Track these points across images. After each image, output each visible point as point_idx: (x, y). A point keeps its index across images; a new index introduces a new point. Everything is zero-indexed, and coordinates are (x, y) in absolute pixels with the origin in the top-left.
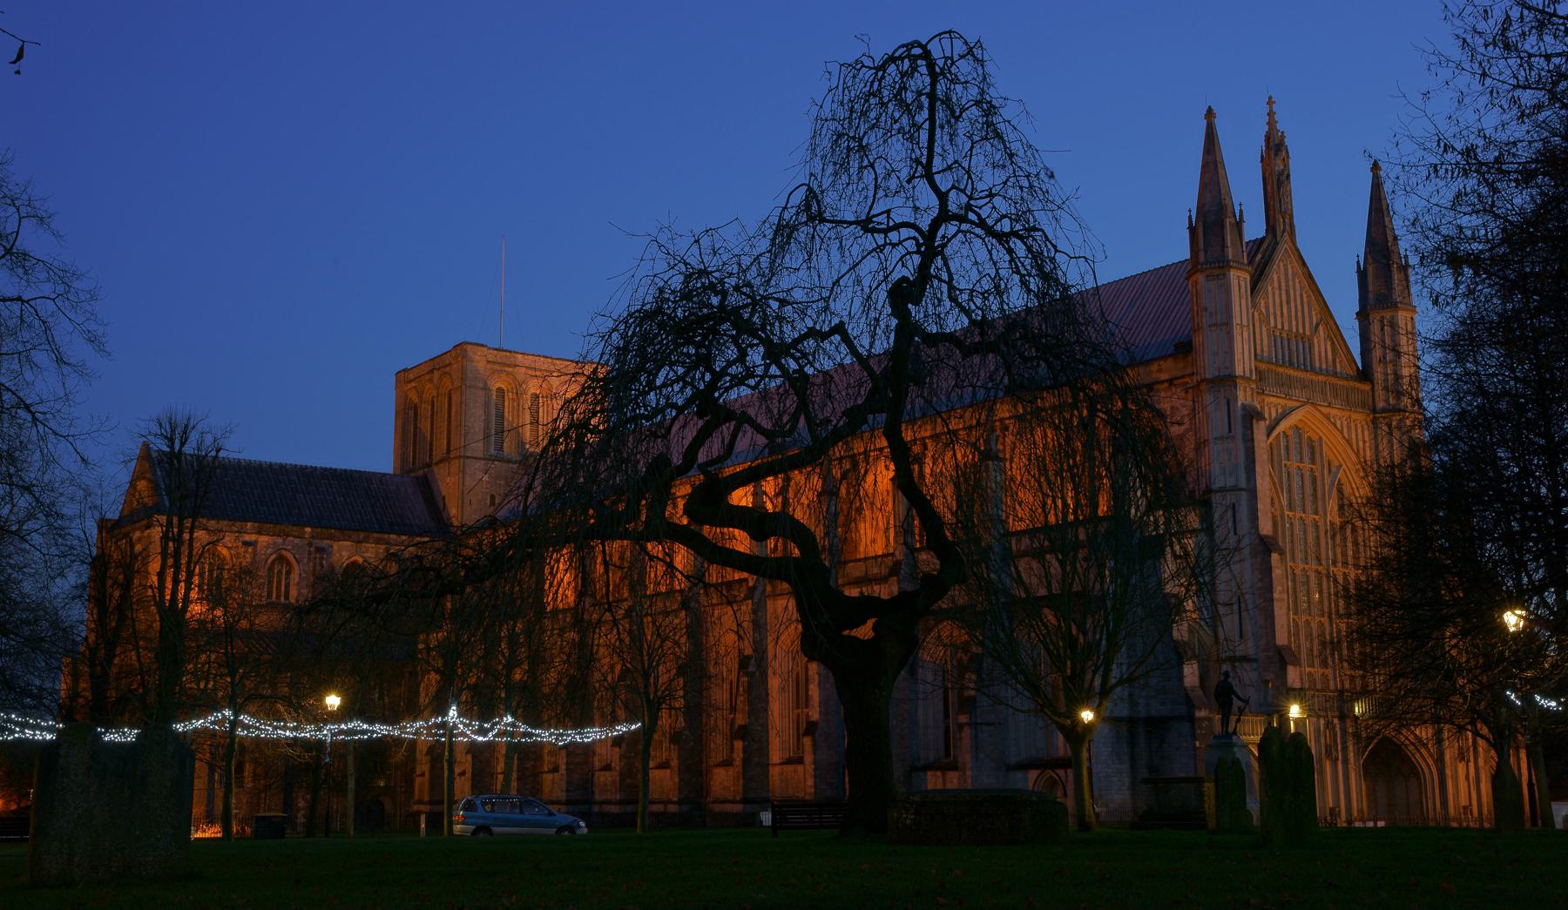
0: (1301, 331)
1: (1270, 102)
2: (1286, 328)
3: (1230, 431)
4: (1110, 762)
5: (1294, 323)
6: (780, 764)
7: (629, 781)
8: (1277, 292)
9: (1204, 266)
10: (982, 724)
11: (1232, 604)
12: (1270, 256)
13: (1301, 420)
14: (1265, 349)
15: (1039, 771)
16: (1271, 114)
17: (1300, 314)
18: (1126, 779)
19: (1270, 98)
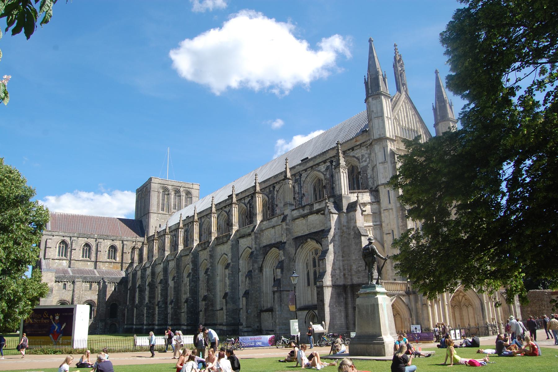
0: (413, 128)
1: (395, 45)
2: (407, 126)
3: (385, 160)
4: (335, 306)
5: (410, 124)
6: (219, 310)
7: (175, 317)
8: (402, 112)
9: (371, 94)
10: (283, 291)
11: (390, 233)
12: (399, 99)
14: (399, 133)
15: (307, 311)
17: (412, 122)
18: (343, 314)
19: (395, 44)
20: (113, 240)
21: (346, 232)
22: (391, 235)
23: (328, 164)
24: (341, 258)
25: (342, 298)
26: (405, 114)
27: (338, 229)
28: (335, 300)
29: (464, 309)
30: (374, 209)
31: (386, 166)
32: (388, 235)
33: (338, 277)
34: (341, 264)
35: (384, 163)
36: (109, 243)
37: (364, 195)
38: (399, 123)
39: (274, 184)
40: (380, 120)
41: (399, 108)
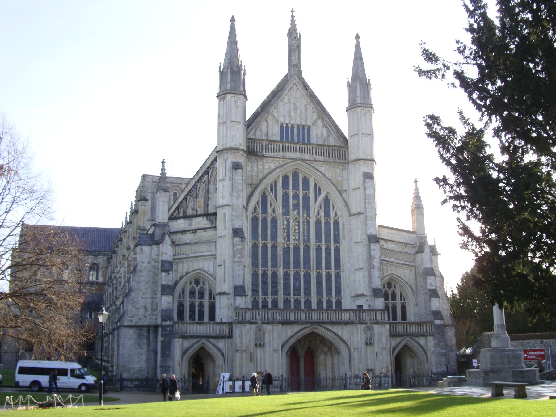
3: (225, 176)
4: (133, 348)
11: (221, 265)
13: (297, 168)
16: (293, 17)
20: (96, 256)
21: (154, 266)
22: (223, 266)
23: (207, 176)
24: (149, 296)
25: (145, 340)
26: (292, 106)
27: (149, 263)
28: (134, 342)
29: (336, 357)
30: (208, 236)
31: (225, 183)
32: (220, 267)
33: (142, 317)
34: (149, 301)
35: (224, 180)
36: (90, 261)
37: (194, 221)
38: (277, 121)
39: (186, 195)
40: (225, 126)
41: (280, 100)
